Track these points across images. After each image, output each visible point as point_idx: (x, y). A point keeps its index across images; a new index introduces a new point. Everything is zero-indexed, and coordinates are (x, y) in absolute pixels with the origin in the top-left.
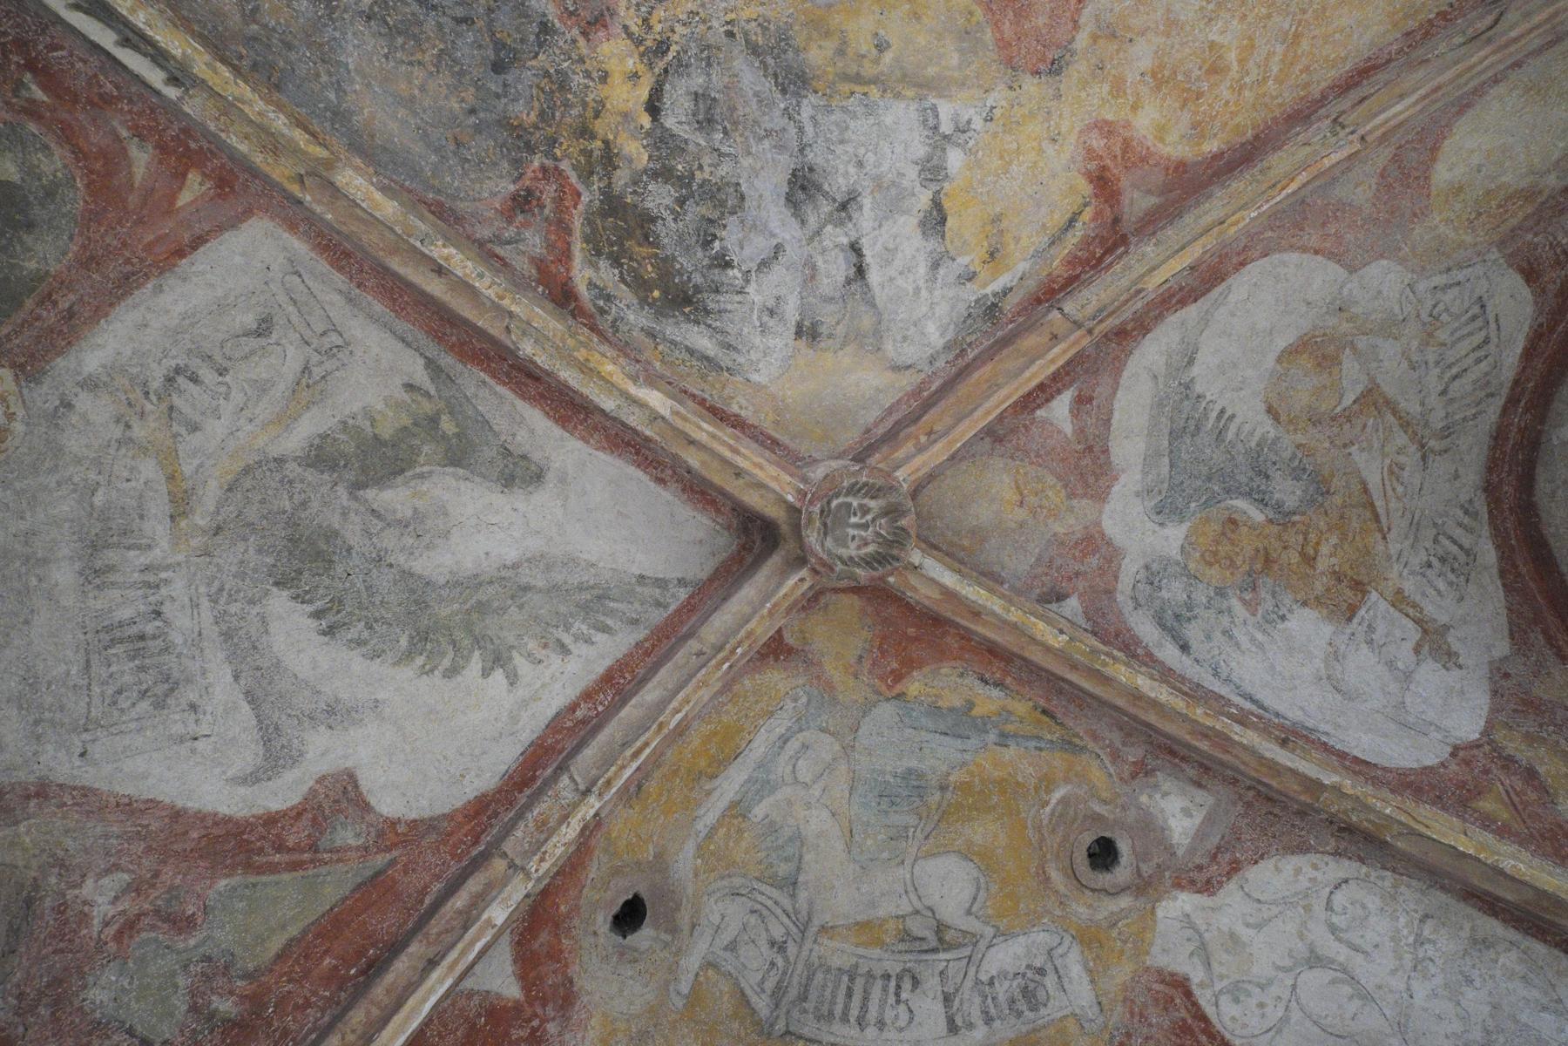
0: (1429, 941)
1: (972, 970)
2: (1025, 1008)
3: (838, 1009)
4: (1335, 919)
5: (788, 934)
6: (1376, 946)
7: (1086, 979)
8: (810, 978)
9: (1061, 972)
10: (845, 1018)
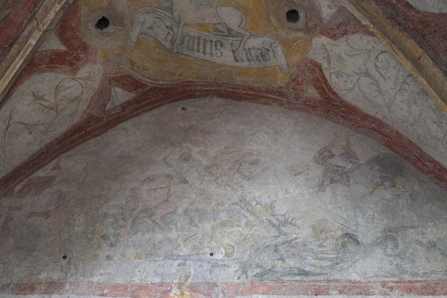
0: (408, 84)
1: (242, 45)
2: (262, 60)
3: (196, 48)
4: (378, 63)
5: (173, 24)
6: (389, 78)
7: (283, 56)
8: (184, 38)
9: (275, 52)
10: (198, 51)
